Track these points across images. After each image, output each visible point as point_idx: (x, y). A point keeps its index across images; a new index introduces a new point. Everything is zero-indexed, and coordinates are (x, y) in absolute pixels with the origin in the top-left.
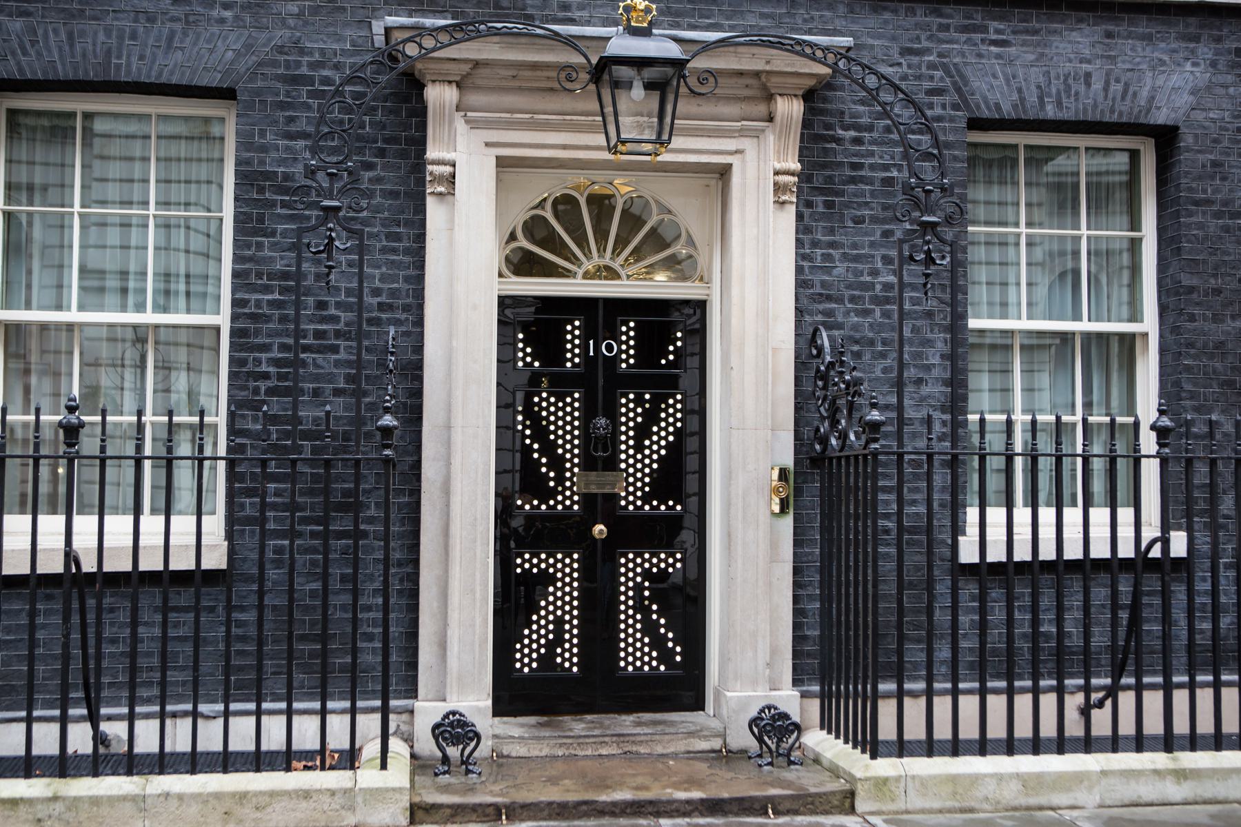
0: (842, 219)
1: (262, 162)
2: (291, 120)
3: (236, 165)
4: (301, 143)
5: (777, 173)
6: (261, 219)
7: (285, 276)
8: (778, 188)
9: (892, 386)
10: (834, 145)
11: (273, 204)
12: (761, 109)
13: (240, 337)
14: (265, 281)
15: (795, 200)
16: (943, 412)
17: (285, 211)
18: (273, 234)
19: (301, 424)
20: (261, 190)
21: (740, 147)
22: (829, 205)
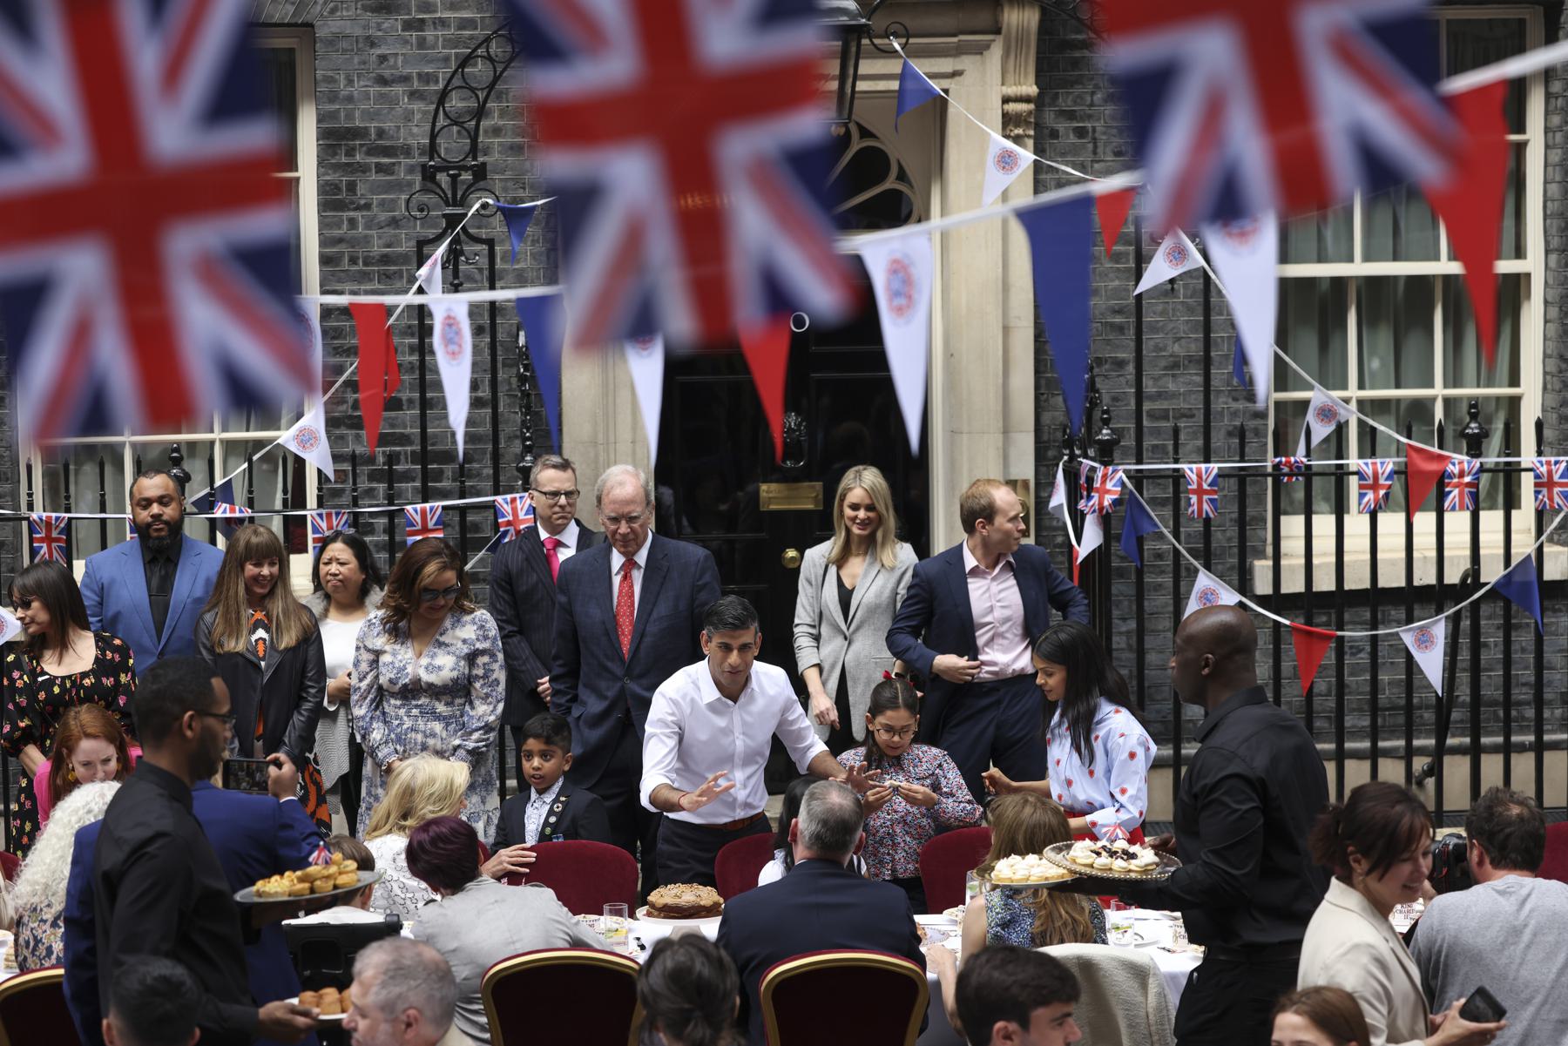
0: (1095, 153)
1: (350, 116)
2: (383, 58)
3: (319, 121)
4: (399, 89)
5: (1006, 100)
6: (352, 187)
7: (385, 259)
8: (1008, 121)
9: (1166, 368)
10: (1086, 53)
11: (364, 169)
12: (983, 18)
13: (333, 338)
14: (360, 266)
15: (1032, 133)
16: (1235, 399)
17: (382, 177)
18: (367, 207)
19: (411, 443)
20: (350, 152)
21: (959, 67)
22: (1081, 132)
